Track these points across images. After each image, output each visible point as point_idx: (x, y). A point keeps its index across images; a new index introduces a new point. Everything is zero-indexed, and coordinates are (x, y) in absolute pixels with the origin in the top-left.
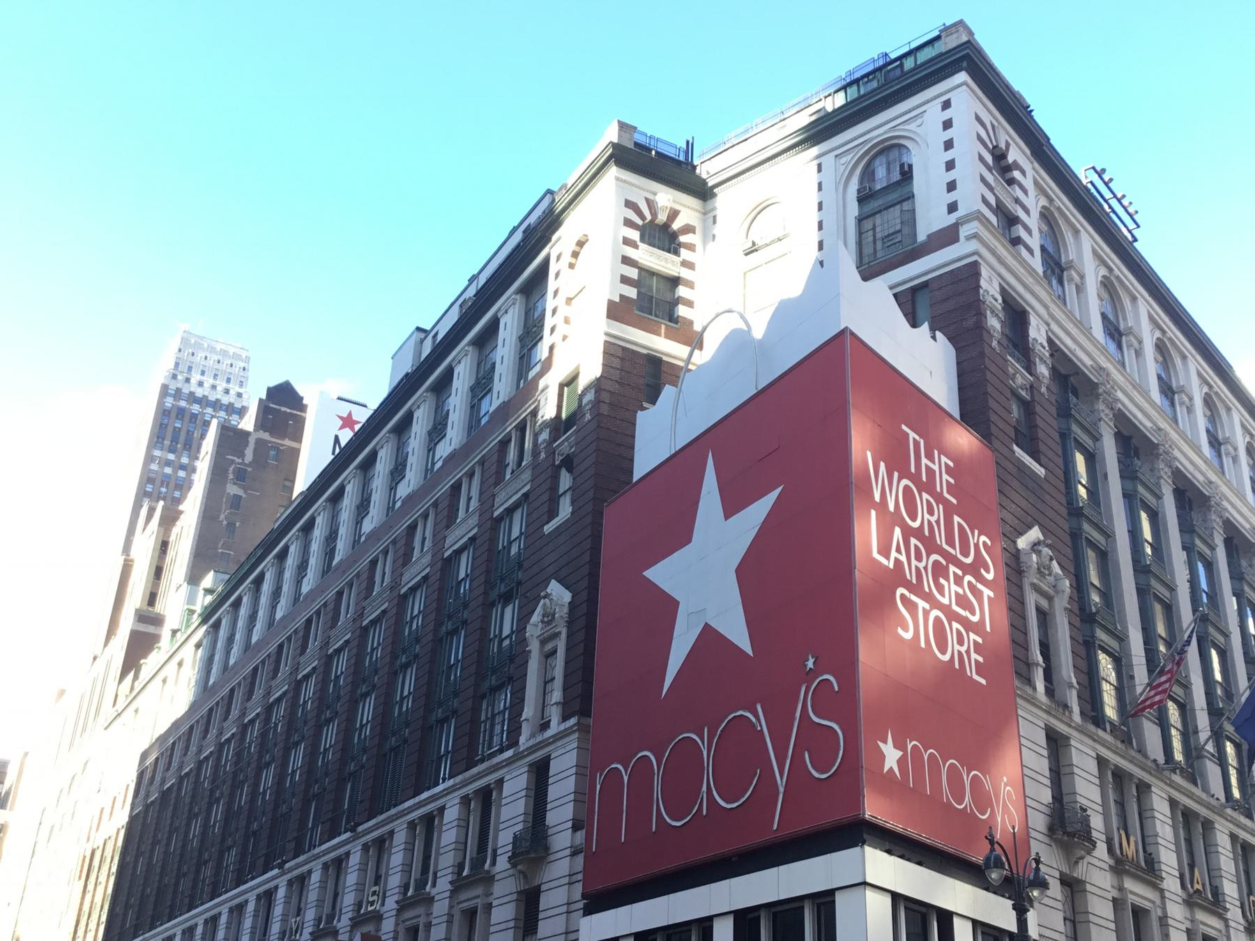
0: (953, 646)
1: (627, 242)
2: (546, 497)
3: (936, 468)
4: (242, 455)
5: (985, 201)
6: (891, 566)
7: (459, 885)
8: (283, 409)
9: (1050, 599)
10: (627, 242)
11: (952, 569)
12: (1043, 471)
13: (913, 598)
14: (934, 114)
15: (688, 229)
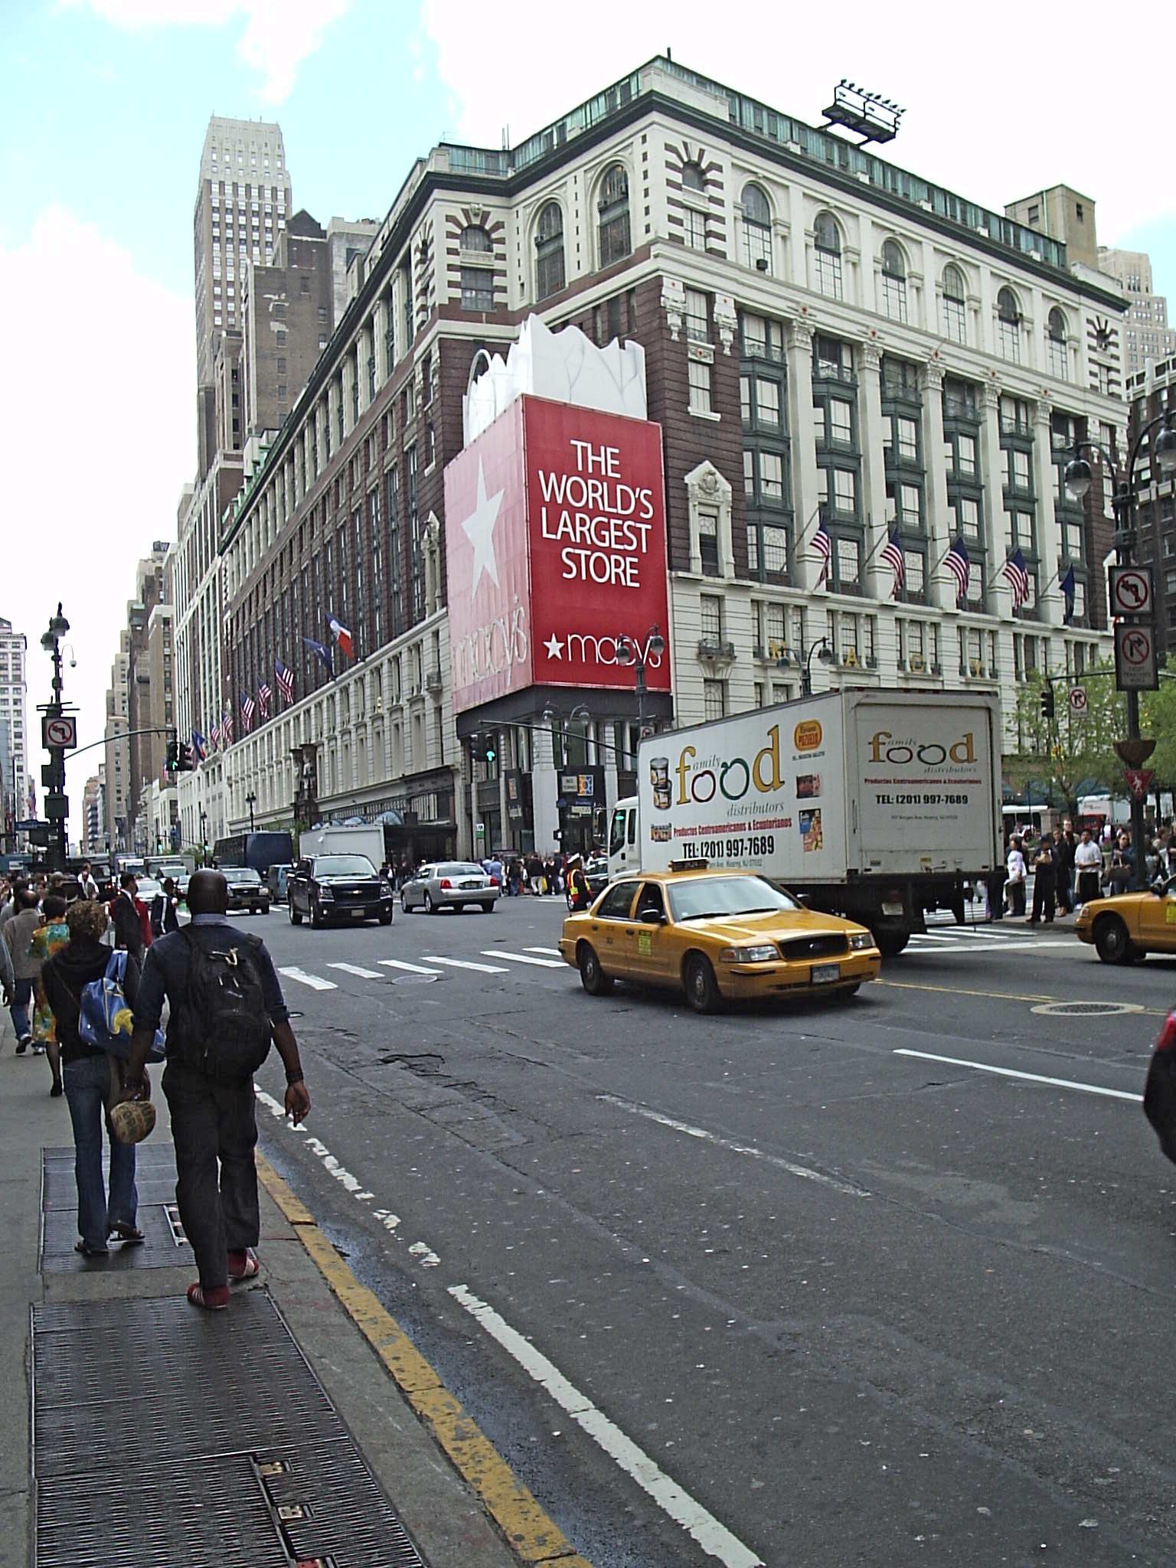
0: (611, 570)
1: (451, 251)
2: (423, 449)
3: (602, 459)
5: (671, 219)
6: (559, 537)
7: (412, 702)
8: (305, 238)
10: (451, 251)
12: (719, 416)
13: (577, 551)
14: (638, 149)
15: (499, 225)
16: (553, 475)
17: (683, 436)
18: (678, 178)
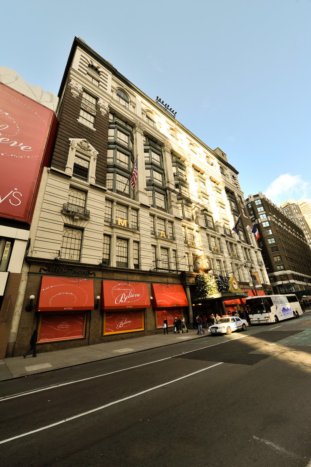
9: (90, 157)
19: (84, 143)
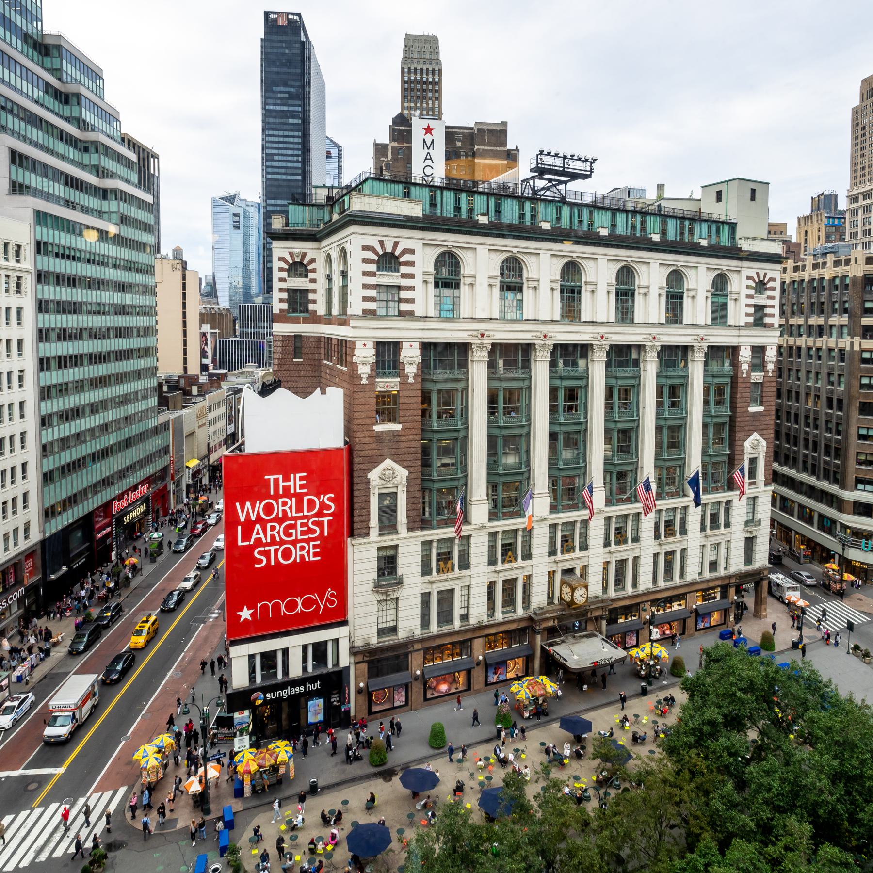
4: (387, 157)
11: (299, 522)
15: (313, 261)
16: (248, 504)
17: (366, 447)
18: (373, 268)
19: (387, 472)
